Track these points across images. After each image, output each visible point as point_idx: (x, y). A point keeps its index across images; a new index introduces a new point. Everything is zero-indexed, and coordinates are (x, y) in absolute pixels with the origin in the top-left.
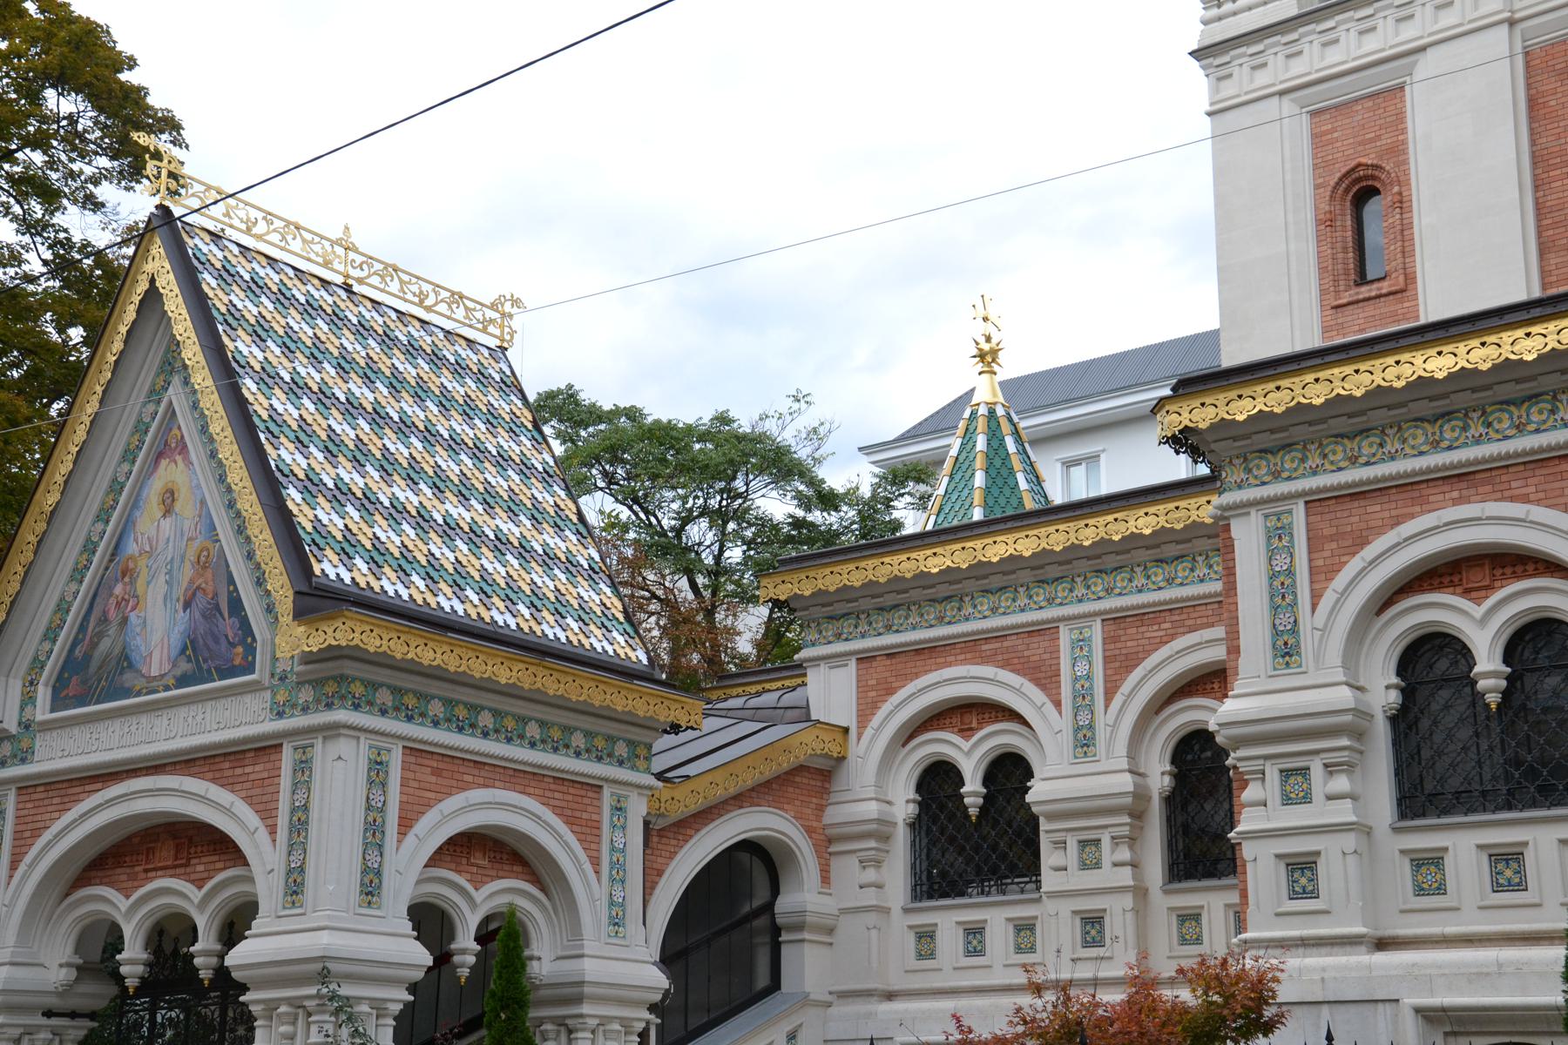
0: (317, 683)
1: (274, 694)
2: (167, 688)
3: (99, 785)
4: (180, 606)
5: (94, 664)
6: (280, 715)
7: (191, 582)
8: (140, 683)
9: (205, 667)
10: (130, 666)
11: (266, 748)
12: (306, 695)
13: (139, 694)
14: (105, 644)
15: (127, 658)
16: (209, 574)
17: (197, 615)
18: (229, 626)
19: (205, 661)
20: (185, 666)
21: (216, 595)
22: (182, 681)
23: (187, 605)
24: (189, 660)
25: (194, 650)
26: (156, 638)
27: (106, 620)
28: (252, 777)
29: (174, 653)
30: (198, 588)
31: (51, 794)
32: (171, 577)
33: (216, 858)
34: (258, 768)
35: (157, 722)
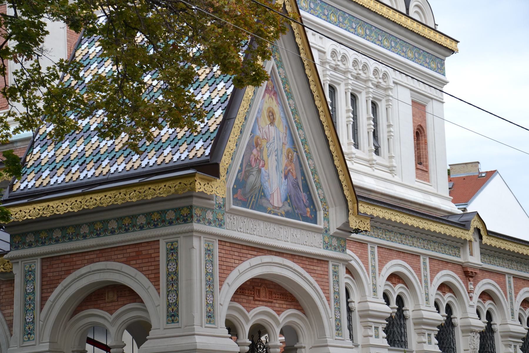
0: (338, 239)
1: (324, 238)
2: (282, 215)
3: (255, 253)
4: (283, 175)
5: (248, 187)
6: (327, 248)
7: (286, 166)
8: (270, 208)
9: (296, 211)
10: (265, 196)
11: (322, 261)
12: (335, 242)
13: (270, 212)
14: (252, 179)
15: (263, 191)
16: (293, 165)
17: (291, 185)
18: (303, 196)
19: (296, 209)
20: (288, 208)
21: (296, 178)
22: (288, 214)
23: (286, 177)
24: (289, 206)
25: (290, 199)
26: (275, 186)
27: (251, 165)
28: (317, 272)
29: (283, 198)
30: (289, 170)
31: (233, 249)
32: (278, 158)
33: (283, 302)
34: (319, 268)
35: (282, 231)
